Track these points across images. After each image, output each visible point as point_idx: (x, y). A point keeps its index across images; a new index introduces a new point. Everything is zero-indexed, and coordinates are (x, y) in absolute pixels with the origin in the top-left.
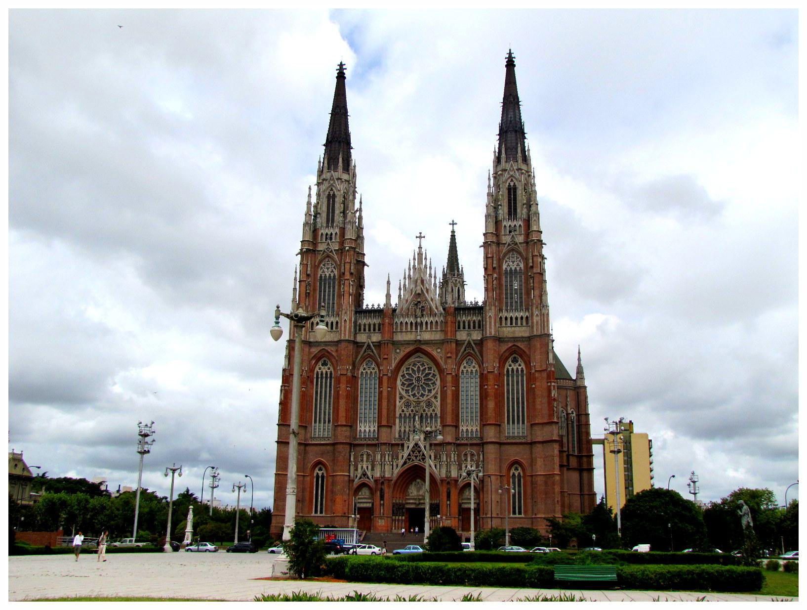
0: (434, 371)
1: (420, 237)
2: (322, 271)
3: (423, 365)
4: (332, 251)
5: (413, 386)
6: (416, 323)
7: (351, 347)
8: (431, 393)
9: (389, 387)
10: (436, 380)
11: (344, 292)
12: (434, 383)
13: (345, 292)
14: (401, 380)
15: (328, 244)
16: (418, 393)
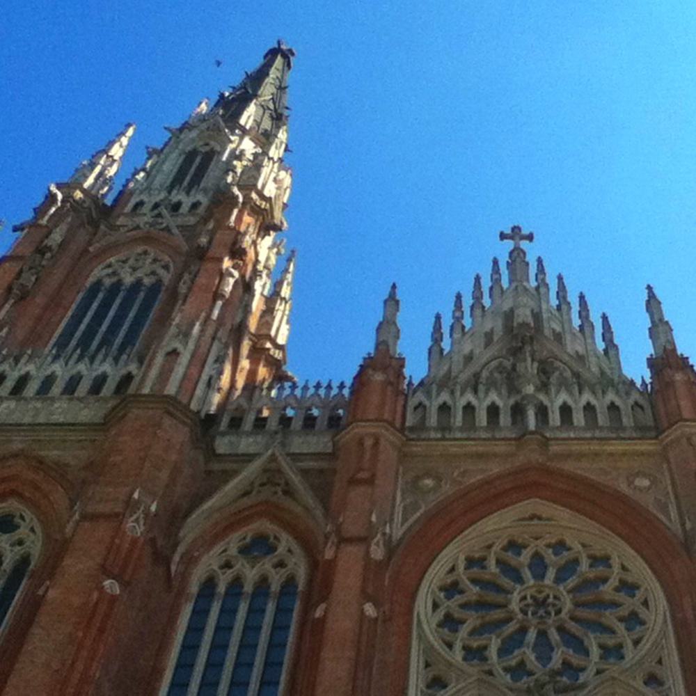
0: (624, 568)
1: (516, 233)
2: (110, 271)
3: (560, 546)
4: (168, 229)
5: (511, 628)
6: (518, 411)
7: (177, 434)
8: (622, 658)
9: (377, 605)
10: (645, 603)
11: (190, 289)
12: (633, 620)
13: (195, 289)
14: (436, 606)
15: (159, 215)
16: (544, 658)
